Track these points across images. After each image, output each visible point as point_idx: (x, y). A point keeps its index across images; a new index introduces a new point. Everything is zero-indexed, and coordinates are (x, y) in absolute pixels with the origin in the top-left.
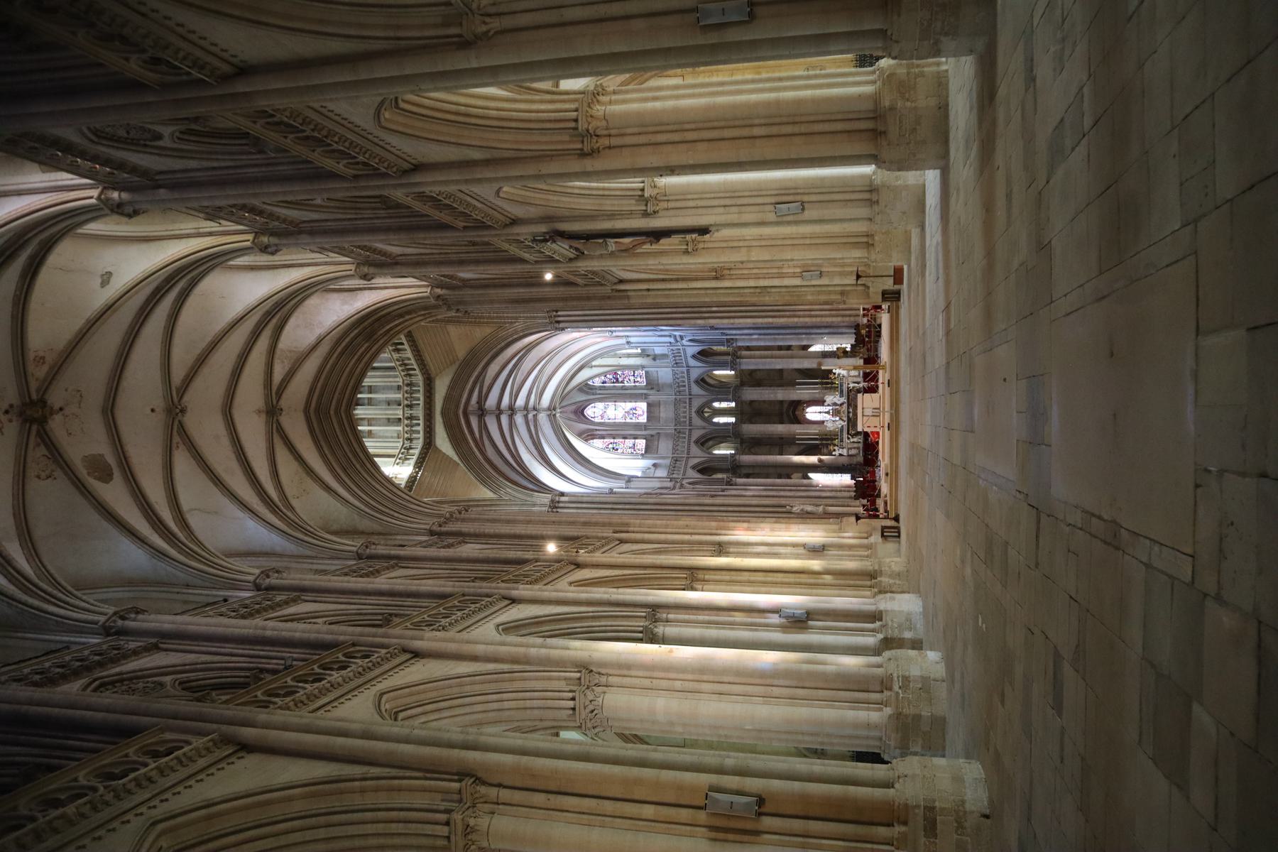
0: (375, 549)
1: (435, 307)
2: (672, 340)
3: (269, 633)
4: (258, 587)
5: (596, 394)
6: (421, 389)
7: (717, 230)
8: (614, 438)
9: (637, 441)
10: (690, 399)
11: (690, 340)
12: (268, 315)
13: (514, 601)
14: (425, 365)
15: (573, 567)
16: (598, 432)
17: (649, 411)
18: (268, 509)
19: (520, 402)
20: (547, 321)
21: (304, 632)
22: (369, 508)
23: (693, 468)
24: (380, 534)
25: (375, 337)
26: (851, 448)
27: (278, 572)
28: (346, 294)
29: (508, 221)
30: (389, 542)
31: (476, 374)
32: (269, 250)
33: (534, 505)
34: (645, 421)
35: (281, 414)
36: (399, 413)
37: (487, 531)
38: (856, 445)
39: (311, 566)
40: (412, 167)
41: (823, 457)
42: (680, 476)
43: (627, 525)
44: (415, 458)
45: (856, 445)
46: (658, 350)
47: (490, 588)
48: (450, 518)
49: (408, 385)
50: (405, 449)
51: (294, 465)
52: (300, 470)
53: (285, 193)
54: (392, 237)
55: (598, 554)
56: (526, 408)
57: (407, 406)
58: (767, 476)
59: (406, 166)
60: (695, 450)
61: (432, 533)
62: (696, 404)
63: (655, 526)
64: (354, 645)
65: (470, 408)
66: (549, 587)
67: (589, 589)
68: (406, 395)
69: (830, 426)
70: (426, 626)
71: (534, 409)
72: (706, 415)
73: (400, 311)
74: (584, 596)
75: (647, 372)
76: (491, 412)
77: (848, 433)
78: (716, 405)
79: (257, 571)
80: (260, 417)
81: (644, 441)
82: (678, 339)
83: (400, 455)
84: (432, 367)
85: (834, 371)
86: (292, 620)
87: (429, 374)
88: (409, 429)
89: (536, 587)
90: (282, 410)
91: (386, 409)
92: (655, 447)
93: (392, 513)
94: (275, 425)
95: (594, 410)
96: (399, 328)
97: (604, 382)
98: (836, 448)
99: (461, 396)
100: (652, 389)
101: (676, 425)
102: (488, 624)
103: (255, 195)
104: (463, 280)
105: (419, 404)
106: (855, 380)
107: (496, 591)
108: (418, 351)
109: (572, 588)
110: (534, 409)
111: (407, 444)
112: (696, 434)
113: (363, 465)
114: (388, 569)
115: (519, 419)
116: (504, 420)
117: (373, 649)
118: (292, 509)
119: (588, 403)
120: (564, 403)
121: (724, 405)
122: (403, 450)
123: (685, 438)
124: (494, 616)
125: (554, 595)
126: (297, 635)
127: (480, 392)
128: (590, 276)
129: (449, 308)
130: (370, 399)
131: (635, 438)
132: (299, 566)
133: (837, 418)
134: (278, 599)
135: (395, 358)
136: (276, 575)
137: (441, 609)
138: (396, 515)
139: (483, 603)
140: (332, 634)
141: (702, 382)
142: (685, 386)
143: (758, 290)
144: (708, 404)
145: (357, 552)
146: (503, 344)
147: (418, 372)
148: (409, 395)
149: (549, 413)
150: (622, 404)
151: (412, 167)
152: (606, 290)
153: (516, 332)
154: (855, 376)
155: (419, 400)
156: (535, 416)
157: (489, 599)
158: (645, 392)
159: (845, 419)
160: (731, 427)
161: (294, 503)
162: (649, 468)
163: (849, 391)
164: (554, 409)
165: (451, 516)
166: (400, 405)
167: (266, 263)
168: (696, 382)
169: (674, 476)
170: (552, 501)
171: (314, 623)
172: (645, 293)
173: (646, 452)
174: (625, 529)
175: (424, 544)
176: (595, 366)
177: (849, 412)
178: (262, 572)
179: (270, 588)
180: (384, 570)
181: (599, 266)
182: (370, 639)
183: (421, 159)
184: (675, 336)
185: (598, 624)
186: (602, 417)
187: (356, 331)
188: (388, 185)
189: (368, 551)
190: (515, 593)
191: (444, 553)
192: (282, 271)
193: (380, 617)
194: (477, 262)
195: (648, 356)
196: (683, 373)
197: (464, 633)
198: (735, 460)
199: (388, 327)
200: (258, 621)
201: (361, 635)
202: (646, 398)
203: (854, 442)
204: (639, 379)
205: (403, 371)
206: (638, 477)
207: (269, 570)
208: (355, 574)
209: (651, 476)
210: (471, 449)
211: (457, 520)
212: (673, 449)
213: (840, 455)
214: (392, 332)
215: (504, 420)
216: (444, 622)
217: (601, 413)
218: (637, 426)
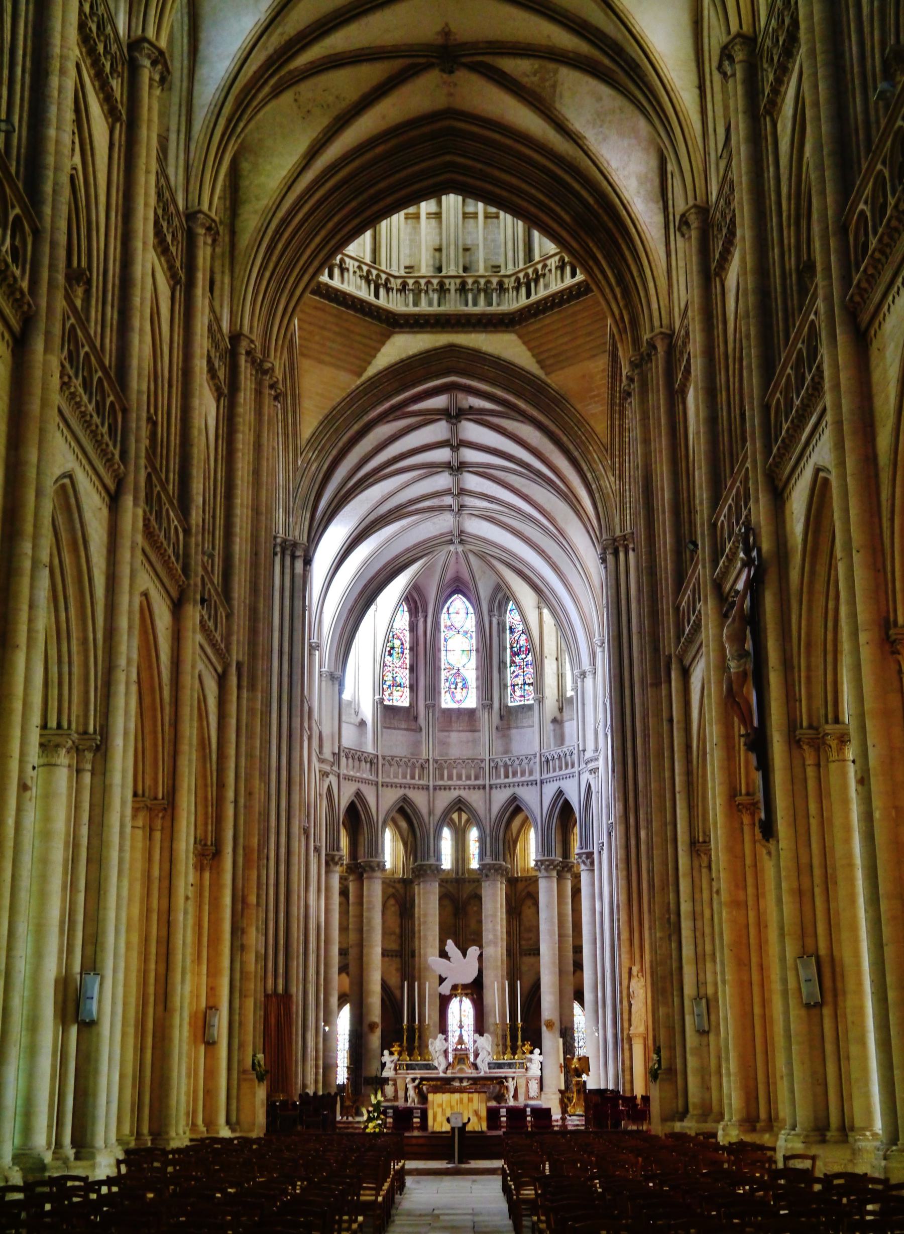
0: (205, 243)
1: (636, 341)
2: (589, 754)
3: (54, 81)
4: (136, 44)
5: (490, 616)
6: (494, 309)
7: (769, 853)
8: (411, 649)
9: (407, 690)
10: (484, 787)
11: (589, 787)
12: (615, 50)
13: (114, 501)
14: (535, 315)
15: (175, 594)
16: (421, 620)
17: (459, 710)
18: (276, 51)
19: (472, 482)
20: (618, 533)
21: (57, 142)
22: (279, 226)
23: (358, 794)
24: (233, 245)
25: (582, 234)
26: (395, 1085)
27: (163, 80)
28: (657, 182)
29: (781, 485)
30: (218, 264)
31: (521, 404)
32: (726, 63)
33: (287, 512)
34: (444, 706)
35: (443, 71)
36: (451, 269)
37: (240, 436)
38: (401, 1094)
39: (173, 127)
40: (863, 326)
41: (378, 1033)
42: (344, 771)
43: (252, 687)
44: (371, 298)
45: (401, 1094)
46: (570, 728)
47: (137, 457)
48: (261, 369)
49: (501, 284)
50: (387, 280)
51: (352, 95)
52: (344, 105)
53: (816, 104)
54: (750, 282)
55: (199, 637)
56: (462, 492)
57: (464, 284)
58: (343, 929)
59: (865, 318)
60: (390, 797)
61: (236, 337)
62: (475, 799)
63: (250, 736)
64: (37, 233)
65: (461, 396)
66: (140, 556)
67: (136, 632)
68: (482, 281)
69: (436, 1045)
70: (70, 352)
71: (462, 507)
72: (455, 816)
73: (628, 277)
74: (123, 623)
75: (530, 707)
76: (454, 432)
77: (422, 1079)
78: (474, 834)
79: (163, 44)
80: (438, 33)
81: (406, 703)
82: (591, 765)
83: (374, 272)
84: (534, 325)
85: (537, 1051)
86: (77, 110)
87: (520, 322)
88: (423, 287)
89: (140, 538)
90: (451, 72)
91: (456, 246)
92: (396, 723)
93: (271, 265)
94: (422, 60)
95: (463, 612)
96: (600, 276)
97: (512, 630)
98: (396, 1057)
99: (482, 379)
100: (501, 717)
101: (436, 761)
102: (71, 457)
103: (812, 53)
104: (683, 392)
105: (467, 305)
106: (522, 1092)
107: (132, 468)
108: (561, 304)
109: (137, 600)
110: (462, 507)
111: (395, 284)
112: (420, 799)
113: (355, 213)
114: (171, 267)
115: (443, 481)
116: (443, 455)
117: (28, 267)
118: (277, 92)
119: (476, 602)
120: (472, 558)
121: (474, 848)
122: (384, 276)
123: (413, 778)
124: (88, 467)
125: (125, 571)
126: (52, 132)
127: (492, 413)
128: (693, 618)
129: (633, 365)
130: (475, 215)
131: (411, 687)
132: (175, 108)
133: (451, 1059)
134: (115, 84)
135: (548, 262)
136: (157, 77)
137: (100, 374)
138: (267, 274)
139: (111, 447)
140: (54, 191)
141: (515, 808)
142: (507, 776)
143: (673, 917)
144: (475, 819)
145: (200, 211)
146: (576, 454)
147: (523, 301)
148: (482, 286)
149: (456, 533)
150: (473, 663)
151: (863, 326)
152: (669, 646)
153: (597, 479)
154: (528, 1091)
155: (475, 304)
156: (449, 508)
157: (117, 457)
159: (449, 1074)
160: (432, 861)
161: (287, 97)
162: (357, 713)
163: (501, 1081)
164: (462, 542)
165: (265, 372)
166: (465, 269)
167: (706, 47)
168: (514, 798)
169: (343, 760)
170: (295, 545)
171: (73, 150)
172: (665, 715)
173: (387, 708)
174: (245, 683)
175: (215, 327)
176: (541, 614)
177: (461, 1080)
178: (161, 53)
179: (134, 69)
180: (168, 262)
181: (707, 636)
182: (46, 261)
183: (875, 345)
184: (596, 759)
185: (75, 648)
186: (450, 627)
187: (591, 201)
188: (831, 285)
189: (202, 231)
190: (128, 501)
191: (200, 365)
192: (693, 78)
193: (84, 264)
194: (712, 420)
195: (561, 710)
196: (531, 773)
197: (58, 419)
198: (373, 870)
199: (599, 256)
200: (75, 52)
201: (53, 245)
202: (484, 706)
203: (407, 1089)
204: (518, 693)
205: (527, 275)
206: (340, 692)
207: (165, 65)
208: (160, 212)
209: (344, 718)
210: (388, 397)
211: (259, 383)
212: (393, 757)
213: (383, 1065)
214: (591, 263)
215: (443, 455)
216: (77, 383)
217: (457, 625)
218: (434, 691)
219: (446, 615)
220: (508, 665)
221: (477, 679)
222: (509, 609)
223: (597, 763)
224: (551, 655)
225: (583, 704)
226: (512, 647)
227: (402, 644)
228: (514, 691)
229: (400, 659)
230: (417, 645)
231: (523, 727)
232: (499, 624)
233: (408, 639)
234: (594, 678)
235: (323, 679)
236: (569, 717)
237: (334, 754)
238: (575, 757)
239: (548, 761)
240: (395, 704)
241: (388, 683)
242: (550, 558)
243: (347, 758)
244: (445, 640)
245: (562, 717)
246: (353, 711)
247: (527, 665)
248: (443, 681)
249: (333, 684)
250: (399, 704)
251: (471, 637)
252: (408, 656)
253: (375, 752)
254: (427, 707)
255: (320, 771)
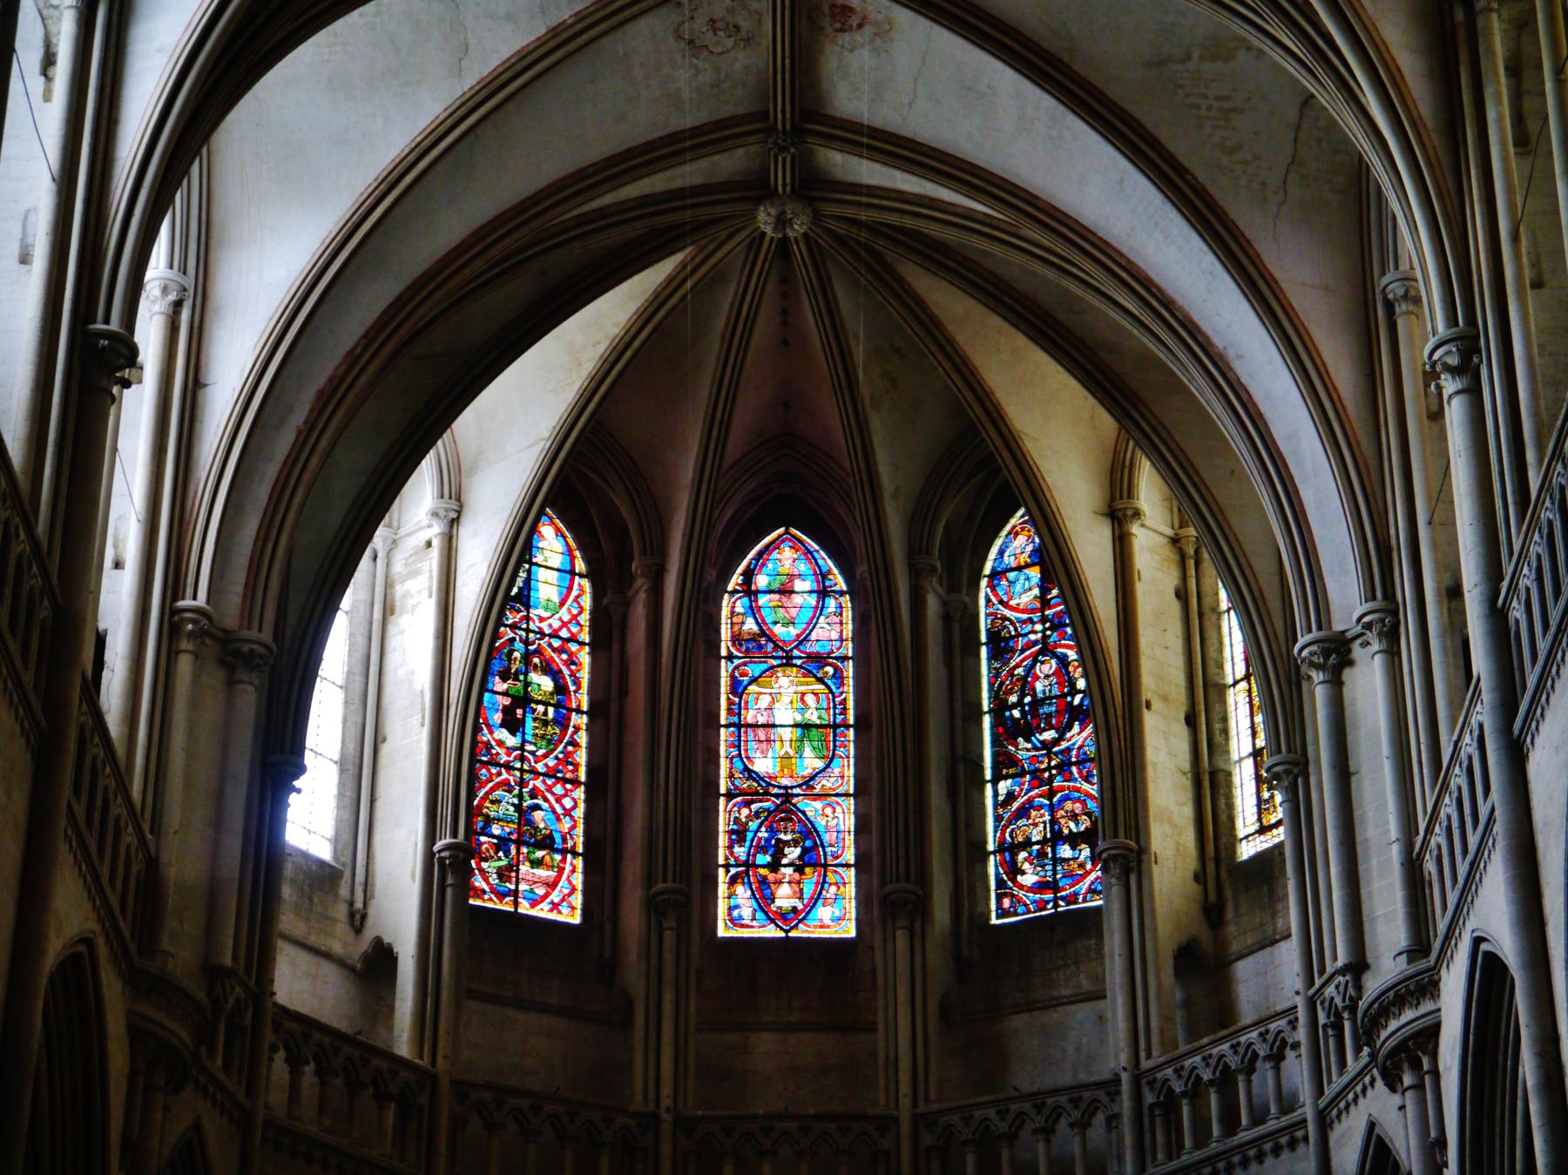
2: (1388, 967)
8: (596, 711)
9: (576, 873)
97: (1001, 646)
150: (844, 774)
158: (941, 913)
162: (358, 920)
184: (1425, 986)
195: (1213, 912)
219: (741, 605)
220: (988, 775)
221: (861, 829)
222: (987, 570)
223: (1426, 1007)
224: (1165, 699)
225: (1344, 774)
226: (999, 707)
227: (561, 688)
228: (1014, 870)
229: (552, 743)
230: (624, 692)
231: (1057, 1003)
232: (947, 619)
233: (585, 675)
234: (1392, 653)
235: (184, 644)
236: (1250, 940)
237: (213, 973)
238: (1297, 1070)
239: (1169, 1105)
240: (525, 908)
241: (496, 830)
242: (1182, 170)
243: (294, 1063)
244: (737, 688)
245: (1221, 943)
246: (341, 912)
247: (1064, 767)
248: (723, 840)
249: (231, 683)
250: (542, 912)
251: (839, 676)
252: (582, 738)
253: (425, 1063)
254: (654, 907)
255: (136, 1034)
